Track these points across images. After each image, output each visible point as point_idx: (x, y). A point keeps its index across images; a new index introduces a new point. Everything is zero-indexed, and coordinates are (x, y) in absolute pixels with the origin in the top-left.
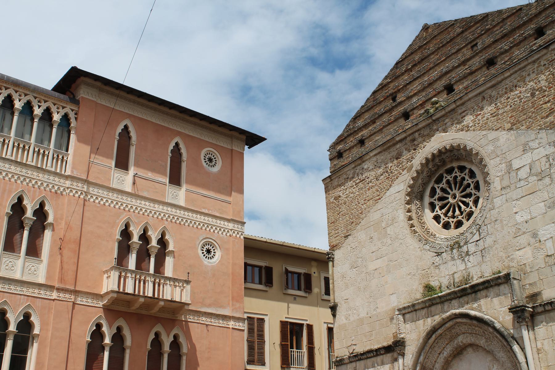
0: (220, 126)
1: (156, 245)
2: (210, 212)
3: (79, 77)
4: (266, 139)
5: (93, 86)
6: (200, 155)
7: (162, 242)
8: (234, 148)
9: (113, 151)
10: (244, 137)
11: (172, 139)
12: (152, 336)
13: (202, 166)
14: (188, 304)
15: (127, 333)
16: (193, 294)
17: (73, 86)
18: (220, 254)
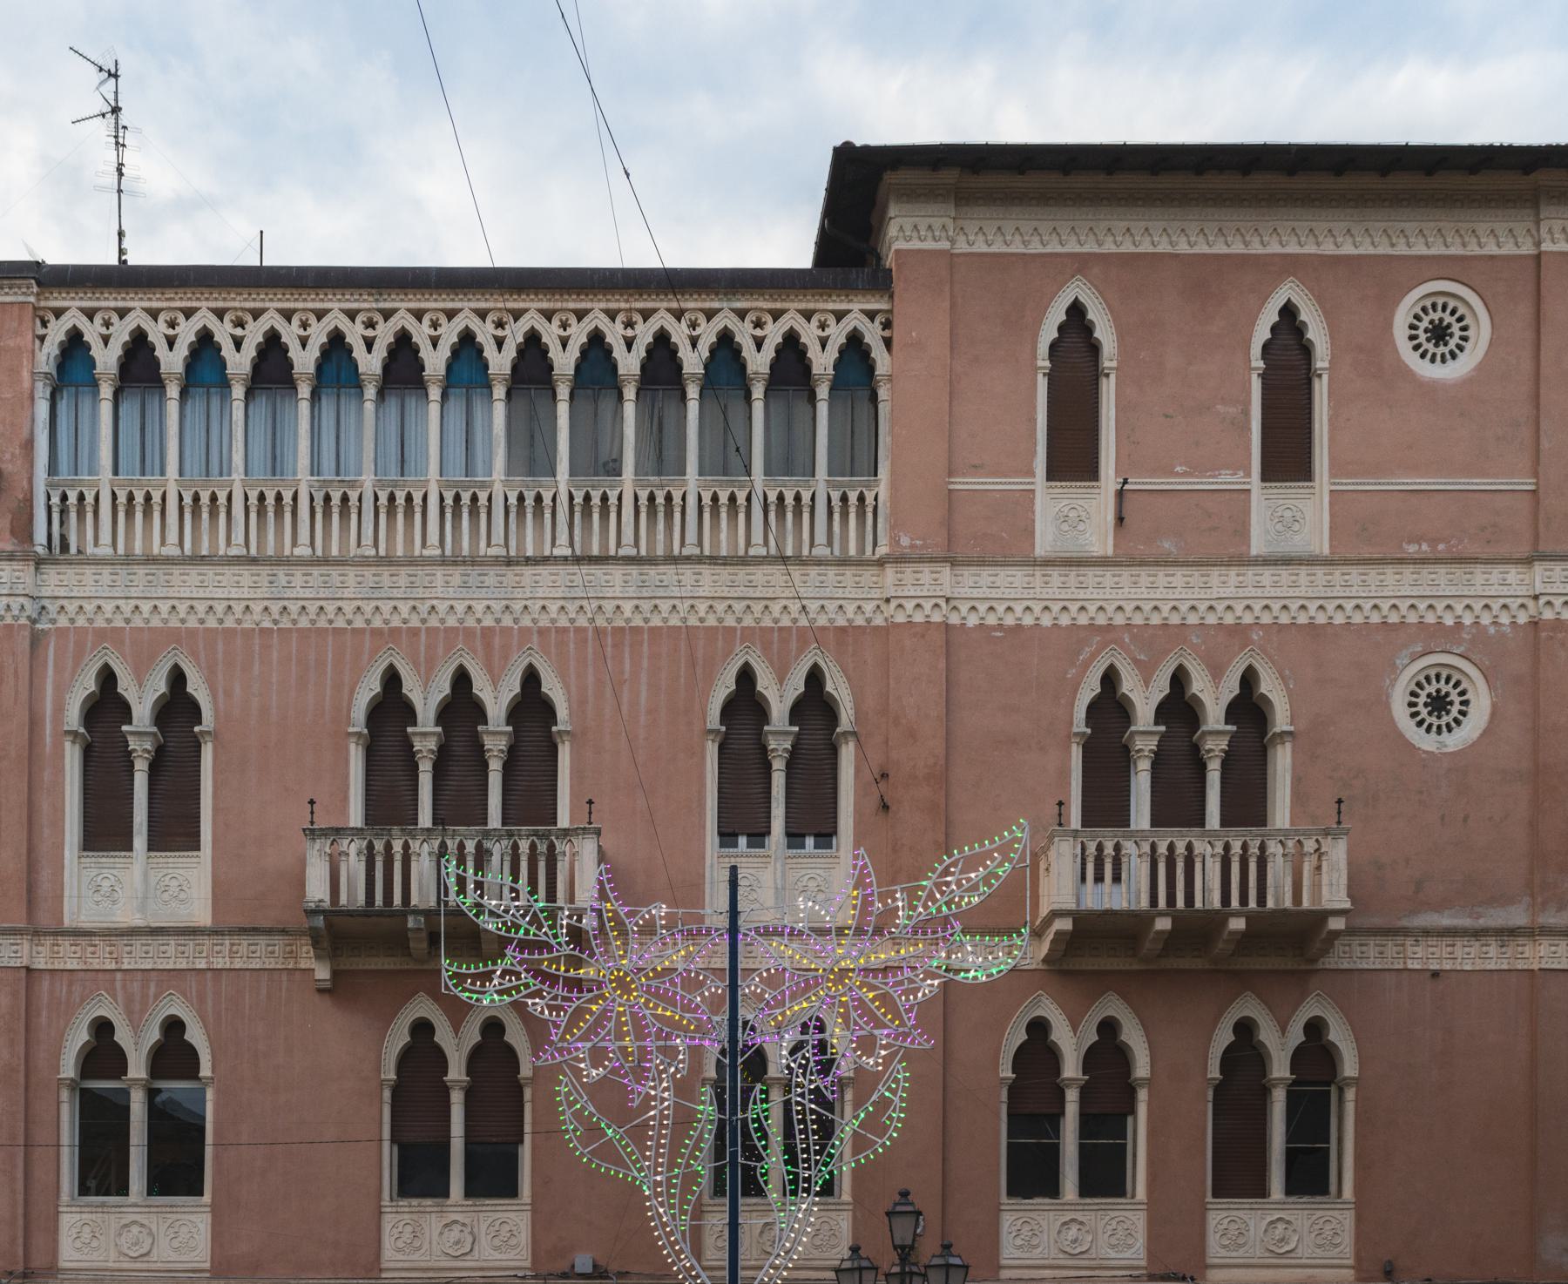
1: (1222, 727)
6: (1389, 325)
8: (1546, 246)
11: (1265, 299)
12: (1224, 1037)
15: (1133, 1036)
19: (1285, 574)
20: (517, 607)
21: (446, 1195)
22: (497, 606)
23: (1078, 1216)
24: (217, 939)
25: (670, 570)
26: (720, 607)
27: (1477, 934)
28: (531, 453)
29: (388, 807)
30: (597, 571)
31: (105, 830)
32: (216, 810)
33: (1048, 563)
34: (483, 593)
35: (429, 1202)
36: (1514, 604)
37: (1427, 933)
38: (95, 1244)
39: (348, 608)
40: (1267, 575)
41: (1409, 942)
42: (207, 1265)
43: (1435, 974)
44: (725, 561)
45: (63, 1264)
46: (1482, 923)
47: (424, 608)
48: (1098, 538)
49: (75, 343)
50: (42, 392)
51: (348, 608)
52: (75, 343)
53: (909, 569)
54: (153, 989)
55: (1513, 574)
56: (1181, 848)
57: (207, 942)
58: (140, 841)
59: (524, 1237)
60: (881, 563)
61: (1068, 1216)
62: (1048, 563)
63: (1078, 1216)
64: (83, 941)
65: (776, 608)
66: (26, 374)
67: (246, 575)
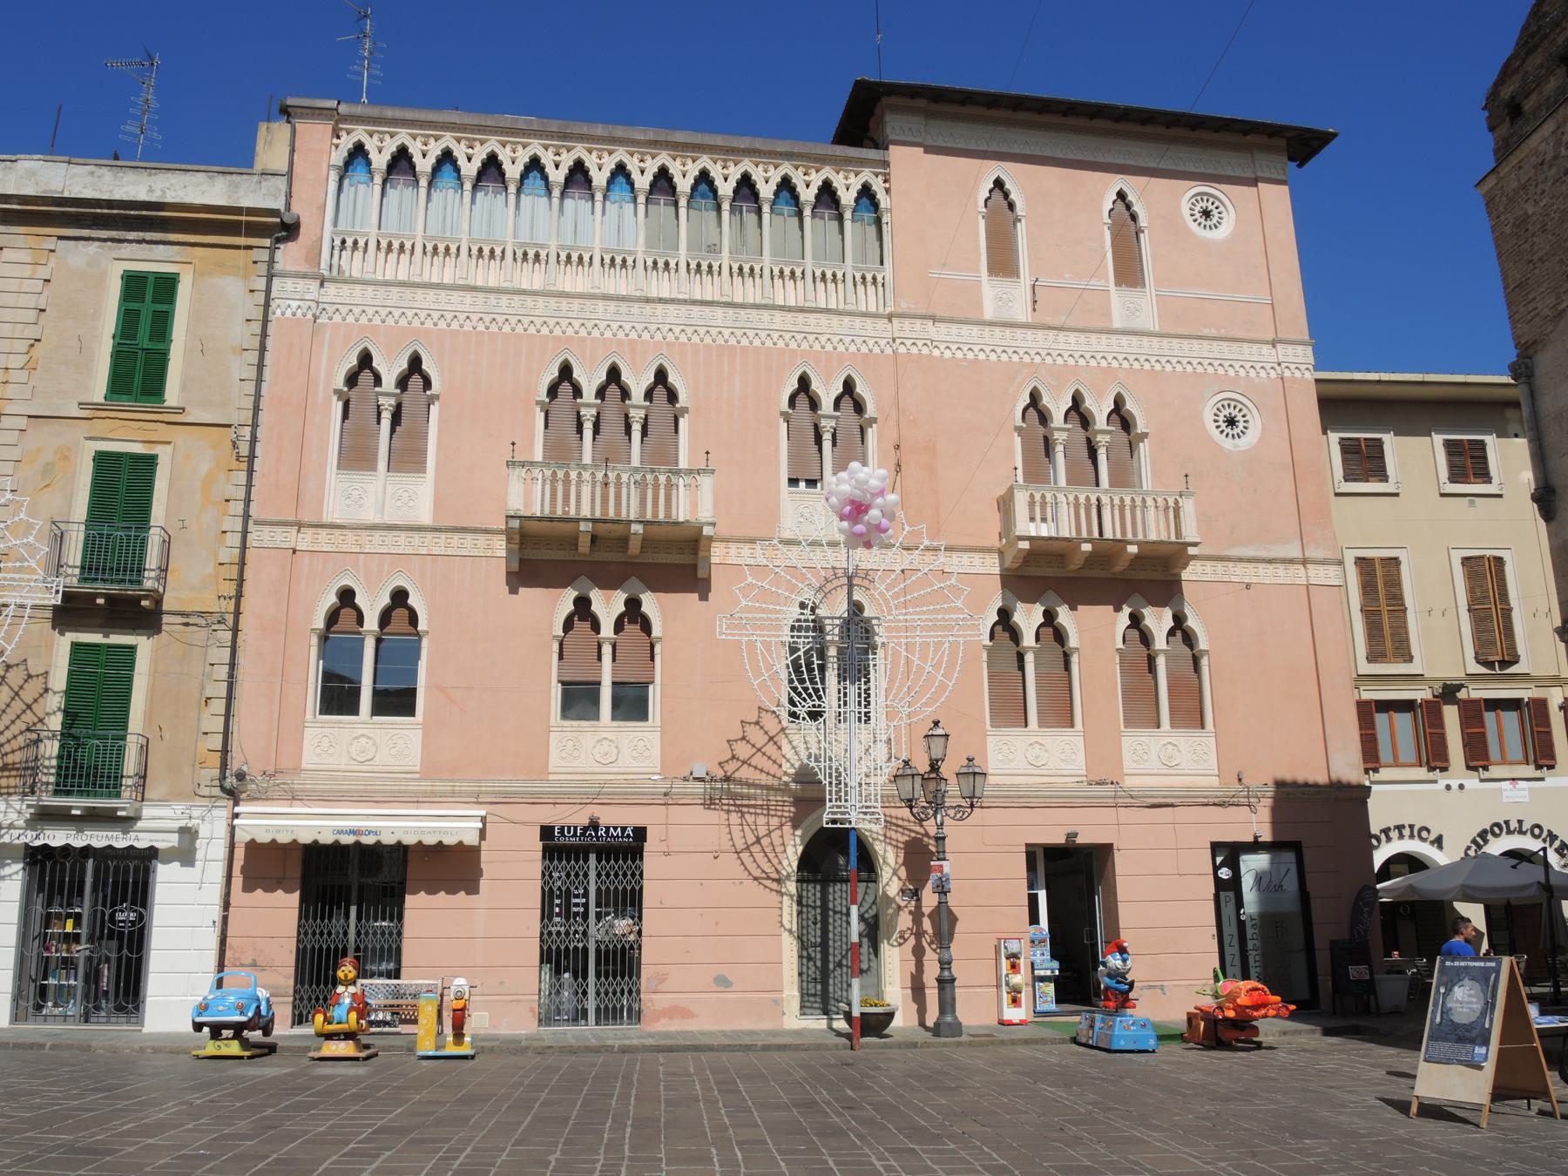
0: (1217, 130)
2: (1223, 333)
3: (878, 99)
4: (1334, 135)
5: (913, 111)
6: (1178, 208)
7: (1121, 417)
9: (977, 241)
10: (1283, 143)
13: (1189, 232)
14: (1195, 544)
16: (1204, 519)
17: (872, 123)
18: (1259, 422)
19: (1134, 339)
20: (653, 328)
21: (597, 718)
22: (640, 327)
23: (1039, 739)
24: (437, 534)
25: (754, 312)
26: (787, 336)
27: (1270, 561)
28: (662, 239)
29: (560, 454)
30: (707, 310)
31: (356, 456)
32: (439, 447)
33: (992, 324)
34: (630, 318)
35: (583, 723)
36: (1268, 366)
37: (1241, 560)
38: (331, 751)
39: (539, 322)
40: (1124, 339)
41: (1231, 564)
42: (418, 768)
43: (1248, 586)
44: (790, 309)
45: (304, 766)
46: (1272, 555)
47: (590, 325)
48: (1022, 313)
49: (359, 151)
50: (333, 177)
51: (539, 322)
52: (359, 151)
53: (907, 321)
54: (386, 568)
55: (1266, 349)
56: (1082, 500)
57: (429, 535)
58: (382, 464)
59: (656, 751)
60: (890, 317)
61: (1034, 739)
62: (992, 324)
63: (1039, 739)
64: (337, 532)
65: (823, 339)
66: (325, 166)
67: (468, 297)
